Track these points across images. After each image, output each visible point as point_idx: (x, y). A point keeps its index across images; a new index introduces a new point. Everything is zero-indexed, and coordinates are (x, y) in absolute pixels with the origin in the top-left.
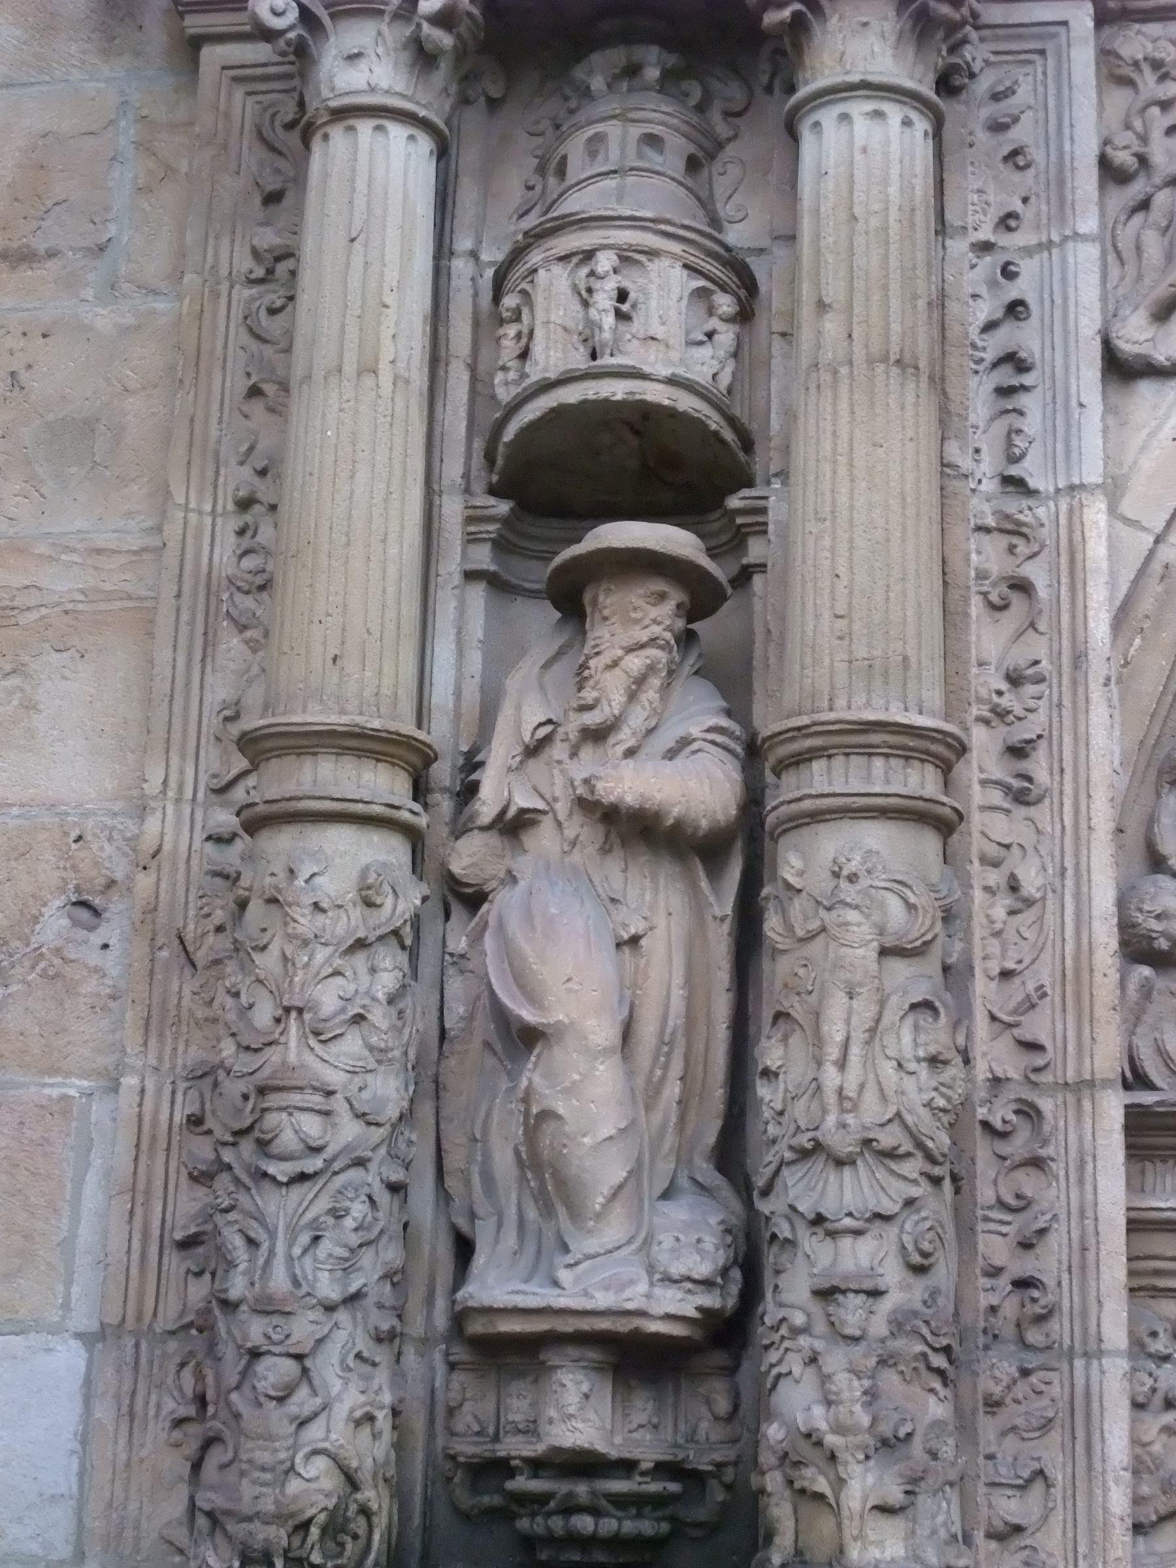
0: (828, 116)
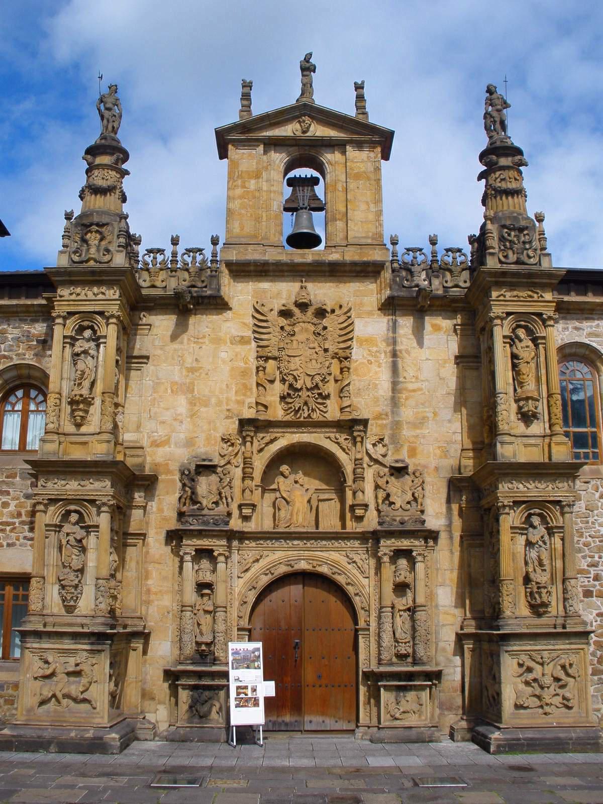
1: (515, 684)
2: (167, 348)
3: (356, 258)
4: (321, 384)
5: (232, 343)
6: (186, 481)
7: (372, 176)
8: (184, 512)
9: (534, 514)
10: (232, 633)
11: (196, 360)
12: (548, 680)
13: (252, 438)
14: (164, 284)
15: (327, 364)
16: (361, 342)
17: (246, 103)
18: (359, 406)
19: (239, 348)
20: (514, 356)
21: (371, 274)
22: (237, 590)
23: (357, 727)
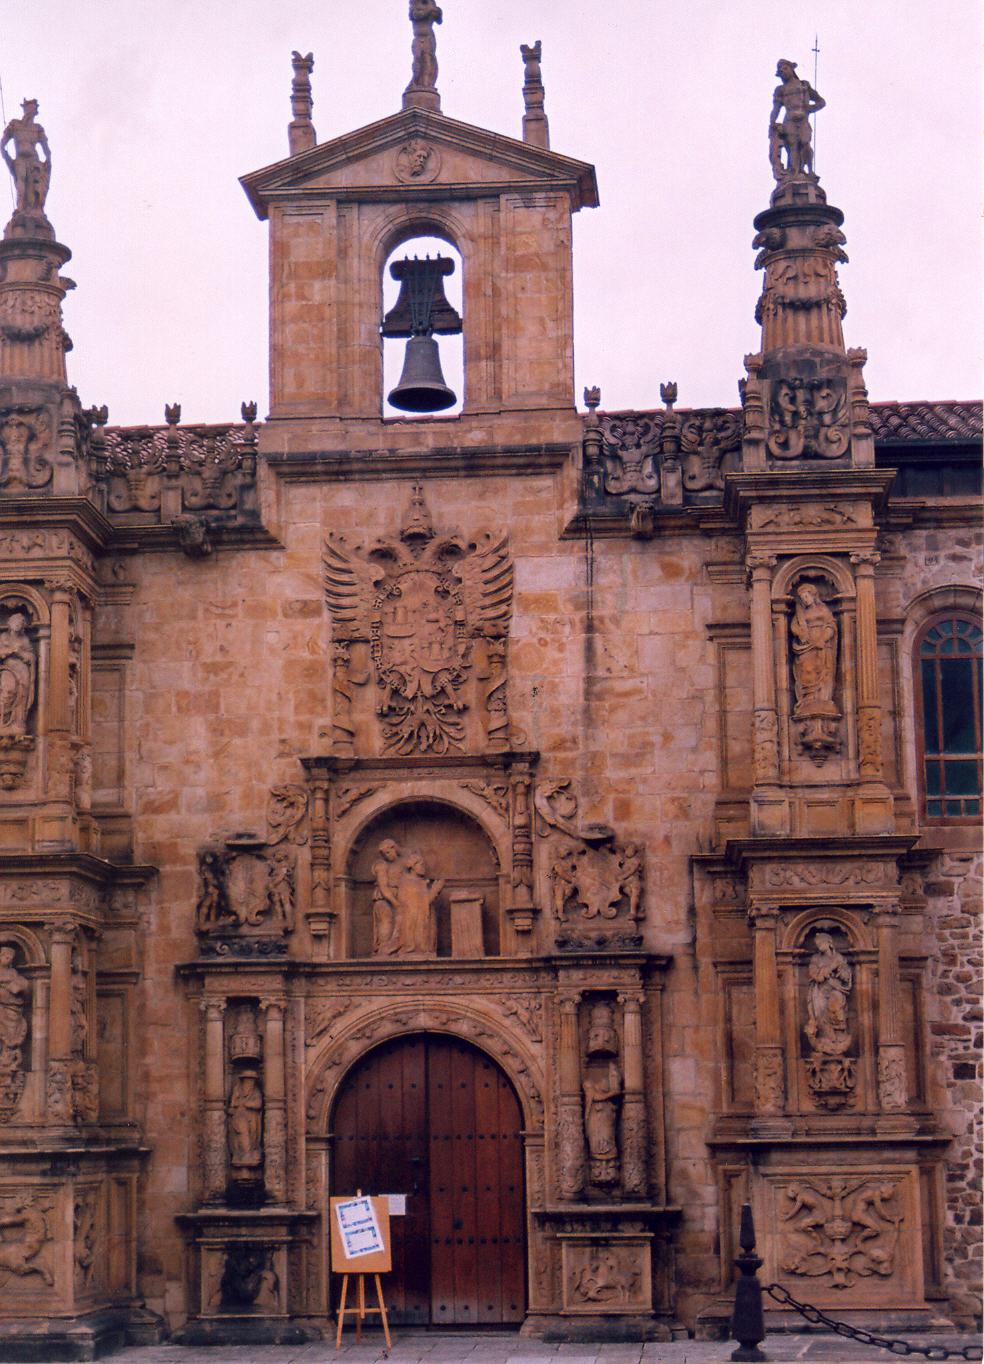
1: (784, 1234)
2: (166, 628)
3: (517, 440)
4: (449, 689)
5: (286, 615)
6: (209, 876)
7: (551, 262)
8: (208, 932)
9: (822, 930)
11: (222, 649)
12: (839, 1227)
13: (327, 792)
14: (156, 502)
15: (461, 649)
16: (528, 604)
17: (301, 106)
18: (522, 726)
19: (300, 625)
20: (792, 638)
21: (546, 470)
23: (526, 1316)
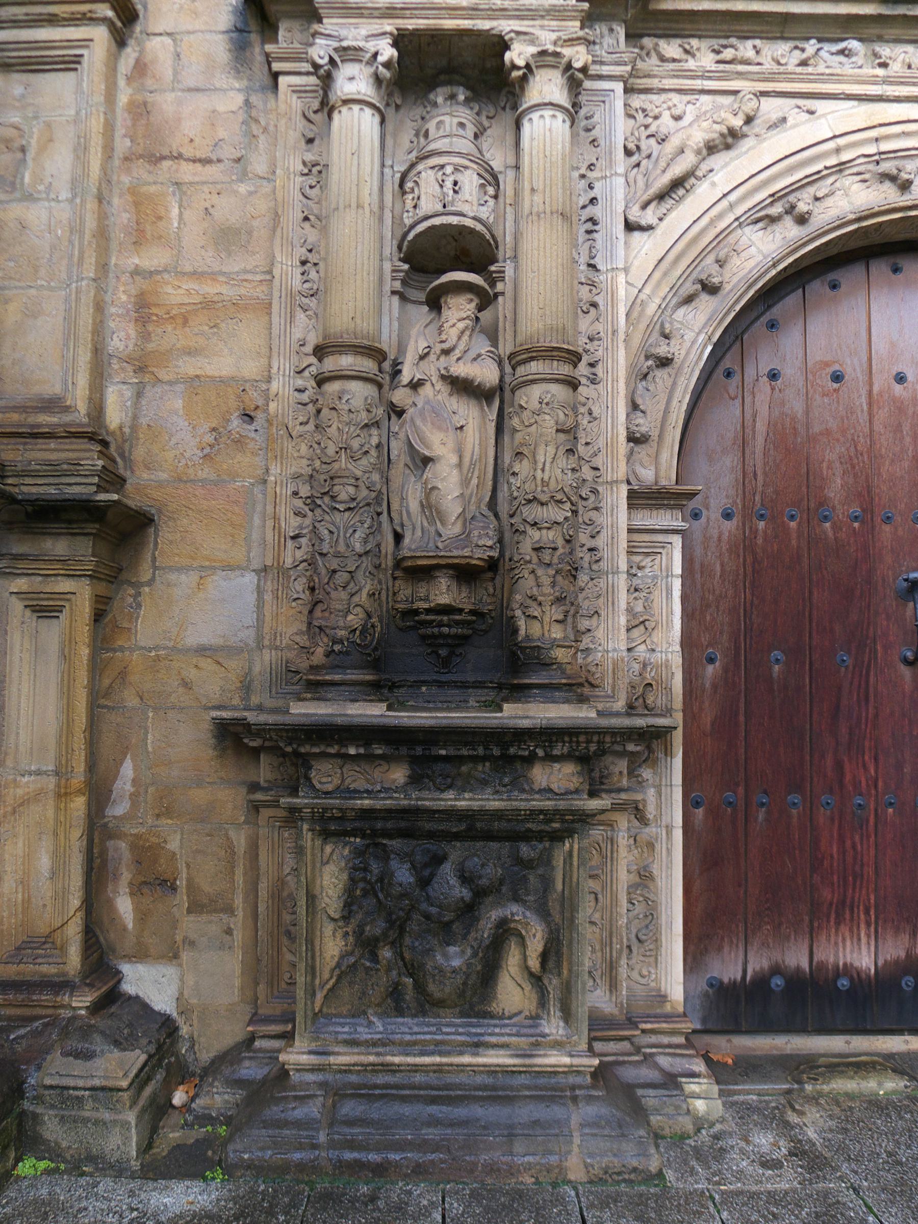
0: (535, 116)
10: (601, 519)
22: (622, 290)
